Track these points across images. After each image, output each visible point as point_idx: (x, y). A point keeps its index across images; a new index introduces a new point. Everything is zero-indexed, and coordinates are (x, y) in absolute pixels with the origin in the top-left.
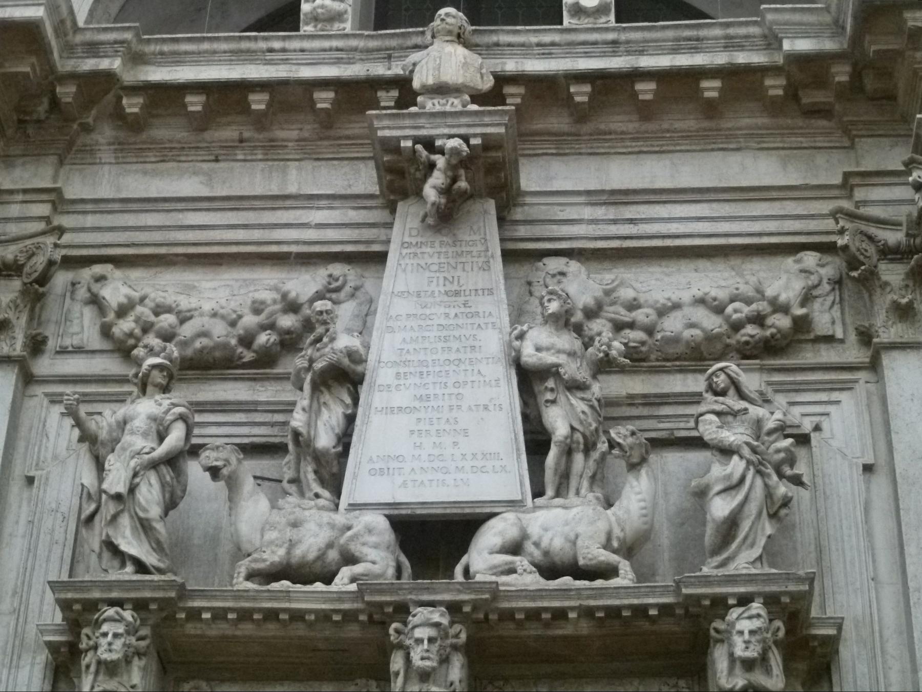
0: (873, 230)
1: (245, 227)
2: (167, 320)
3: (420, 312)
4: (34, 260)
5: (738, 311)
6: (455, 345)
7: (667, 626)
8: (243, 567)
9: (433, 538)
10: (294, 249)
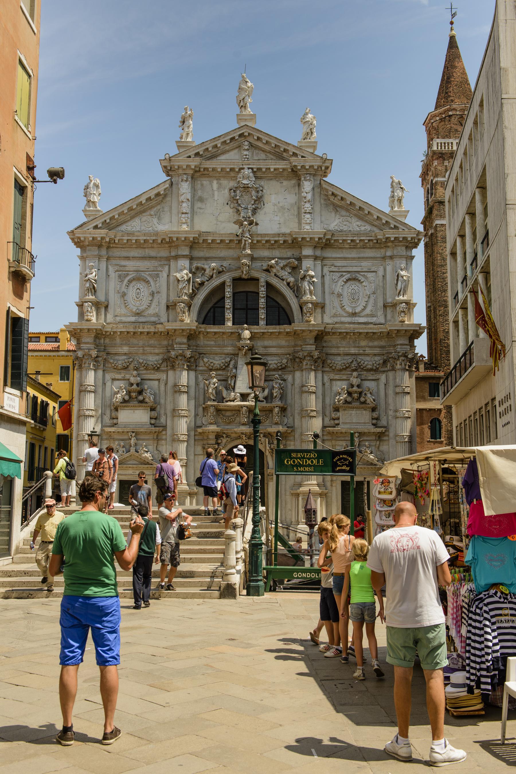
9: (244, 397)
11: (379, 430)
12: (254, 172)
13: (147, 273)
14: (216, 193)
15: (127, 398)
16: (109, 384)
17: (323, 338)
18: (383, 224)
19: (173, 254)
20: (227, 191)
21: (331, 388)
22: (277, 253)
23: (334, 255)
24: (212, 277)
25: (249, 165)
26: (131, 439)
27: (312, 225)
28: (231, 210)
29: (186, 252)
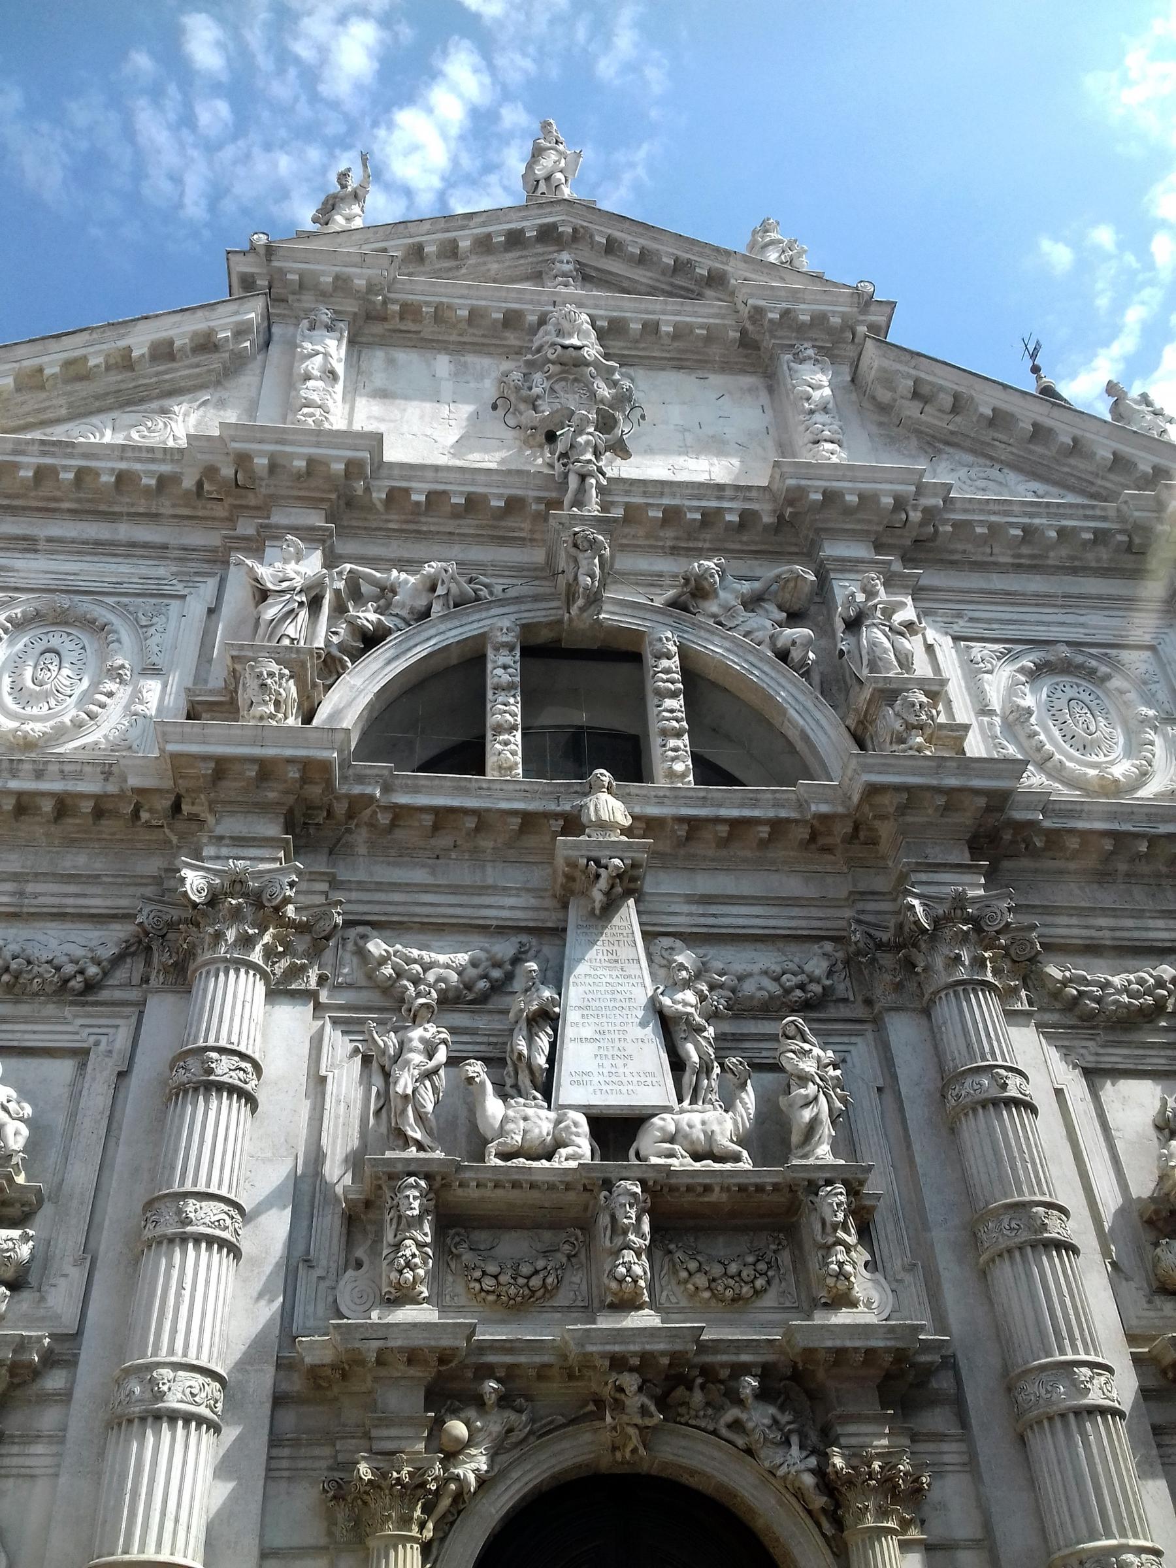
0: (872, 932)
1: (461, 906)
3: (592, 972)
4: (322, 923)
5: (789, 980)
6: (619, 996)
7: (775, 1198)
8: (492, 1148)
9: (615, 1130)
10: (495, 923)
13: (110, 600)
24: (424, 614)
28: (510, 434)
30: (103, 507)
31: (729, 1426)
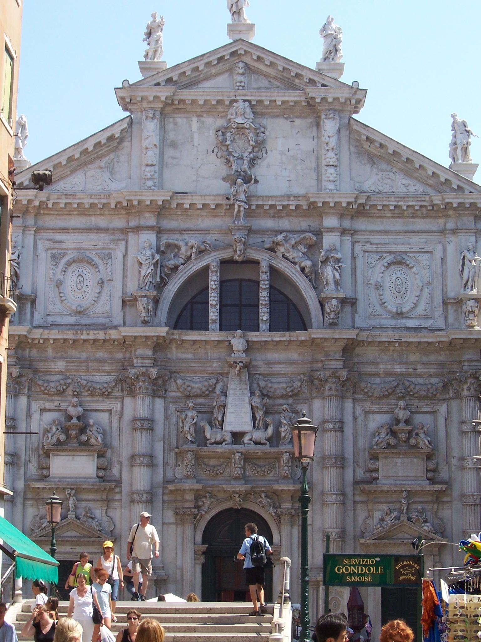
2: (190, 388)
5: (288, 389)
8: (208, 442)
9: (237, 437)
11: (437, 487)
12: (252, 106)
13: (94, 252)
14: (196, 136)
15: (62, 437)
16: (36, 417)
17: (354, 349)
18: (442, 184)
19: (132, 224)
20: (212, 133)
21: (366, 425)
22: (285, 223)
23: (371, 227)
24: (189, 258)
25: (245, 95)
26: (68, 499)
27: (338, 183)
28: (219, 160)
29: (151, 221)
30: (86, 213)
31: (259, 502)
